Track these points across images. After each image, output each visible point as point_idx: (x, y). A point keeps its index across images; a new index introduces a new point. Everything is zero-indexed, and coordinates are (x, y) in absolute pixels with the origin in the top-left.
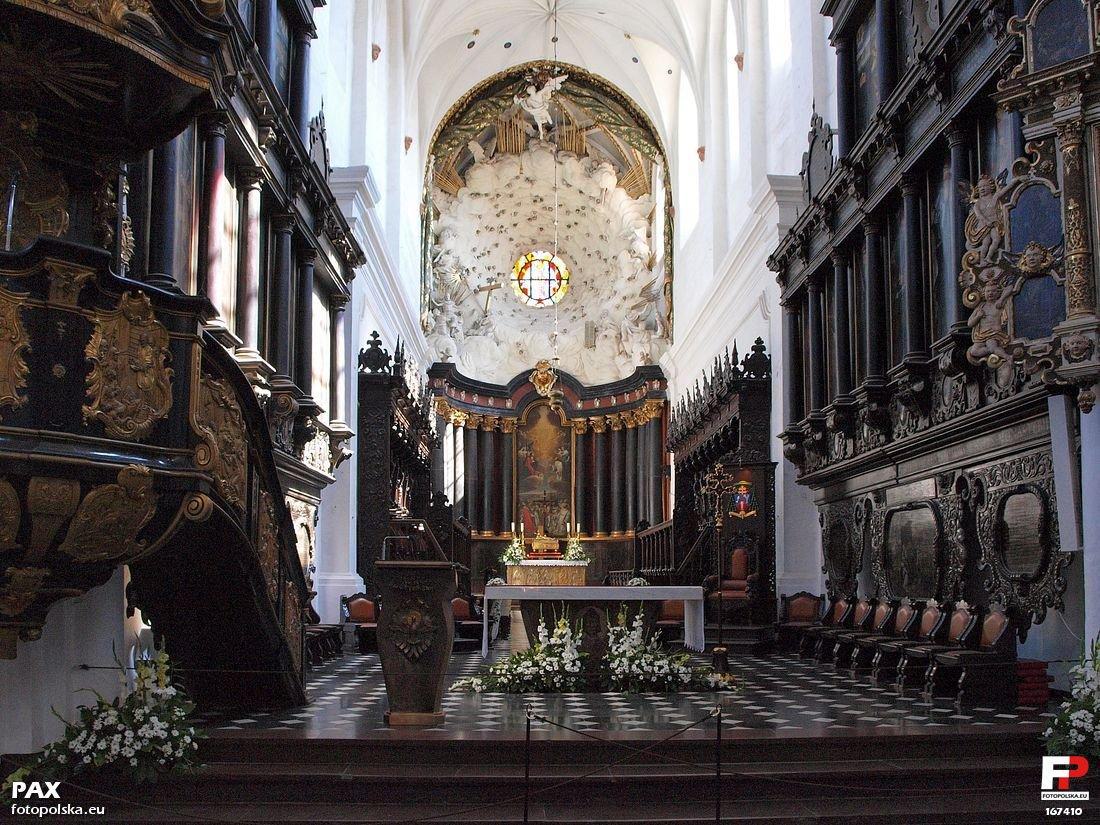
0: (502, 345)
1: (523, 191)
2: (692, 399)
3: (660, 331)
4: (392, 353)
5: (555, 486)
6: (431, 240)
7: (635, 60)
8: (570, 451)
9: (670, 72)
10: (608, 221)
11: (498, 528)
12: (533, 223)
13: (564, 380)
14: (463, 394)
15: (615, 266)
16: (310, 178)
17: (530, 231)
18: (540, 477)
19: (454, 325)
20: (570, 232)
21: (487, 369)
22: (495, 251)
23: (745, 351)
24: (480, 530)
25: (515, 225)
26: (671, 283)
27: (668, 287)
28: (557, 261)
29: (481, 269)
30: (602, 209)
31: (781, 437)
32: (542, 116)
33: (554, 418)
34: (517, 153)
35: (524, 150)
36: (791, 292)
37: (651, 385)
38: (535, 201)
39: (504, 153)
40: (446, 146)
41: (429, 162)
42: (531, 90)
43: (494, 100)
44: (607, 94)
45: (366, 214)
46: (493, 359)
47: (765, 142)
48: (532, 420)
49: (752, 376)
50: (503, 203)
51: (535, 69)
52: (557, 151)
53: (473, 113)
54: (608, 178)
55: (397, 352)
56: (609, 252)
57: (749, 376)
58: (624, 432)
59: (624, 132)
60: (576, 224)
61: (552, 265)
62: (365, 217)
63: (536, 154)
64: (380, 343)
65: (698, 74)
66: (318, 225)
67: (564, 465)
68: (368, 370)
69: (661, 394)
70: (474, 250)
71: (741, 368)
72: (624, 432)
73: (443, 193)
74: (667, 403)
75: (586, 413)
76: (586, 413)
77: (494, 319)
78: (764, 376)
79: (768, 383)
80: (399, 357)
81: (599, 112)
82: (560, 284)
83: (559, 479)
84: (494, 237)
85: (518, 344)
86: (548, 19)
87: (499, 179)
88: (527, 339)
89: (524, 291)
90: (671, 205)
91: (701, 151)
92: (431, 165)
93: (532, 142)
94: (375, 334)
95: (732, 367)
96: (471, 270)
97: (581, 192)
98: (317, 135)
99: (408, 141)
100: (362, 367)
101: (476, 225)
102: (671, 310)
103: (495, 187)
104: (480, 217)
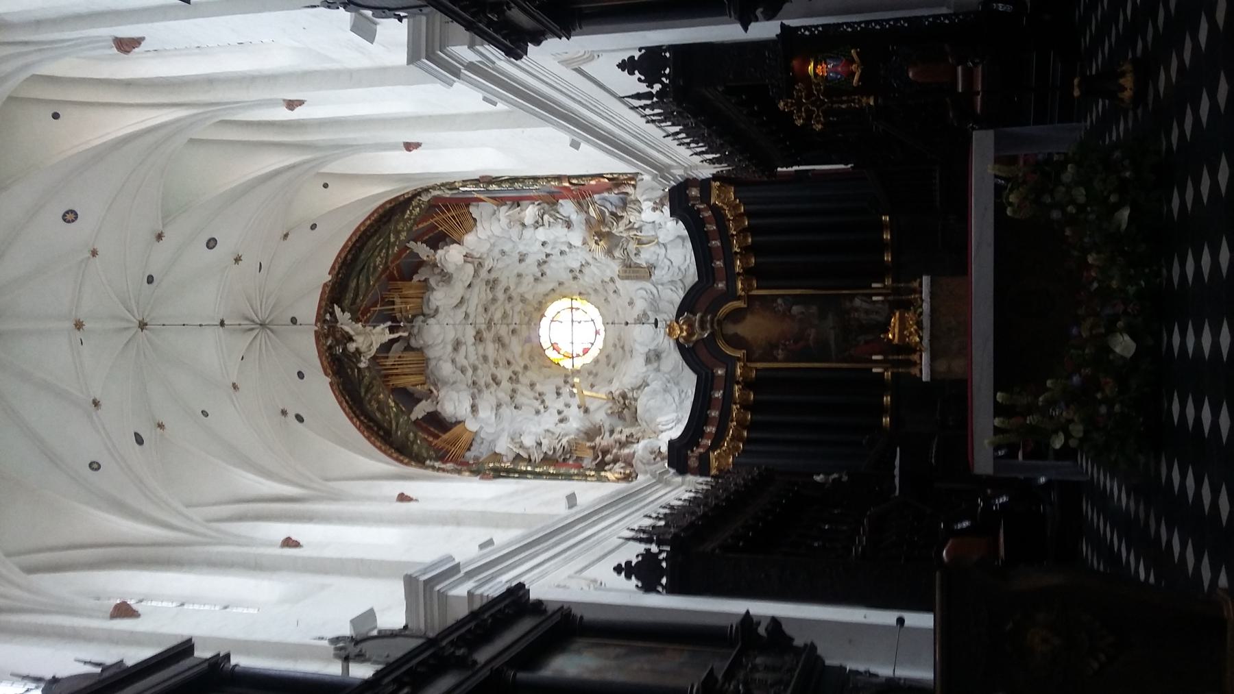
0: (649, 381)
1: (471, 351)
2: (704, 149)
3: (630, 190)
4: (641, 547)
7: (314, 227)
9: (326, 186)
10: (503, 253)
12: (506, 341)
13: (688, 305)
14: (711, 429)
15: (555, 242)
16: (394, 681)
18: (812, 332)
19: (623, 438)
20: (516, 298)
21: (677, 398)
22: (538, 388)
23: (633, 83)
25: (509, 363)
26: (569, 178)
27: (574, 181)
28: (551, 311)
29: (559, 404)
30: (488, 264)
31: (746, 29)
32: (380, 334)
33: (736, 316)
34: (425, 361)
35: (423, 353)
36: (555, 27)
37: (695, 198)
38: (481, 340)
39: (427, 378)
40: (415, 447)
41: (433, 468)
42: (352, 347)
43: (363, 391)
44: (355, 258)
45: (467, 573)
46: (666, 390)
47: (384, 69)
48: (736, 342)
49: (667, 71)
50: (483, 377)
51: (329, 342)
52: (424, 315)
53: (378, 415)
54: (452, 255)
55: (641, 540)
56: (536, 252)
57: (667, 76)
58: (751, 230)
59: (397, 237)
60: (506, 290)
61: (552, 321)
62: (470, 575)
63: (426, 340)
64: (628, 563)
65: (318, 154)
66: (463, 664)
67: (797, 303)
68: (664, 581)
69: (704, 185)
70: (538, 412)
71: (657, 87)
72: (751, 230)
73: (472, 448)
74: (715, 177)
75: (731, 277)
76: (731, 277)
77: (616, 388)
78: (668, 55)
79: (673, 48)
80: (646, 536)
81: (375, 268)
82: (578, 309)
83: (814, 309)
84: (523, 389)
85: (648, 361)
86: (272, 331)
87: (454, 383)
88: (641, 351)
89: (586, 351)
90: (476, 180)
91: (409, 146)
92: (437, 464)
93: (413, 343)
94: (618, 569)
95: (655, 99)
96: (563, 415)
97: (469, 286)
98: (357, 650)
99: (403, 498)
100: (660, 589)
101: (507, 411)
102: (601, 176)
103: (465, 386)
104: (499, 406)
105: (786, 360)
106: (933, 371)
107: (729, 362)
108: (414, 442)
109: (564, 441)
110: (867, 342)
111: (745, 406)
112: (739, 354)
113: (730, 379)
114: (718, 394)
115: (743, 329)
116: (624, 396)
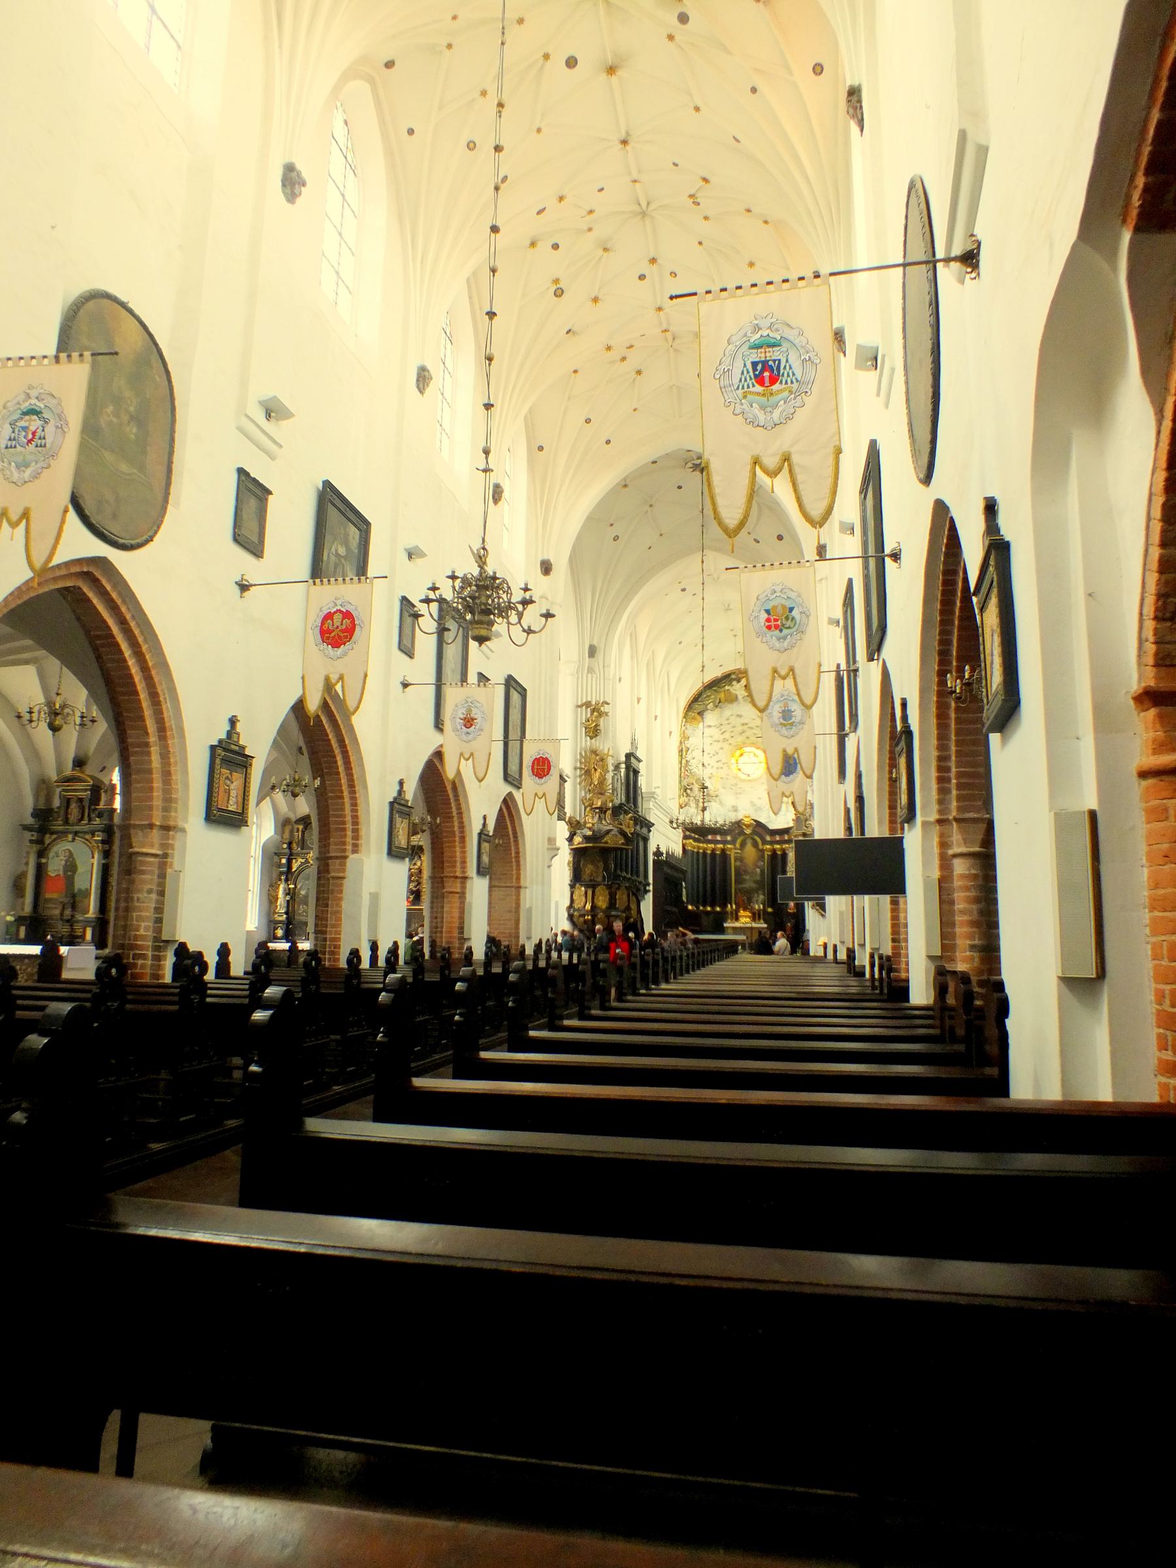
5: (755, 882)
6: (684, 761)
8: (763, 861)
11: (724, 906)
12: (744, 734)
13: (759, 824)
17: (740, 739)
22: (720, 751)
24: (713, 906)
33: (755, 844)
48: (743, 845)
75: (771, 843)
77: (721, 791)
84: (720, 745)
85: (733, 807)
89: (739, 770)
99: (671, 733)
105: (735, 867)
106: (727, 928)
107: (733, 842)
108: (693, 712)
109: (695, 770)
110: (743, 900)
111: (713, 850)
112: (738, 846)
113: (724, 842)
114: (718, 838)
115: (749, 847)
116: (717, 796)
